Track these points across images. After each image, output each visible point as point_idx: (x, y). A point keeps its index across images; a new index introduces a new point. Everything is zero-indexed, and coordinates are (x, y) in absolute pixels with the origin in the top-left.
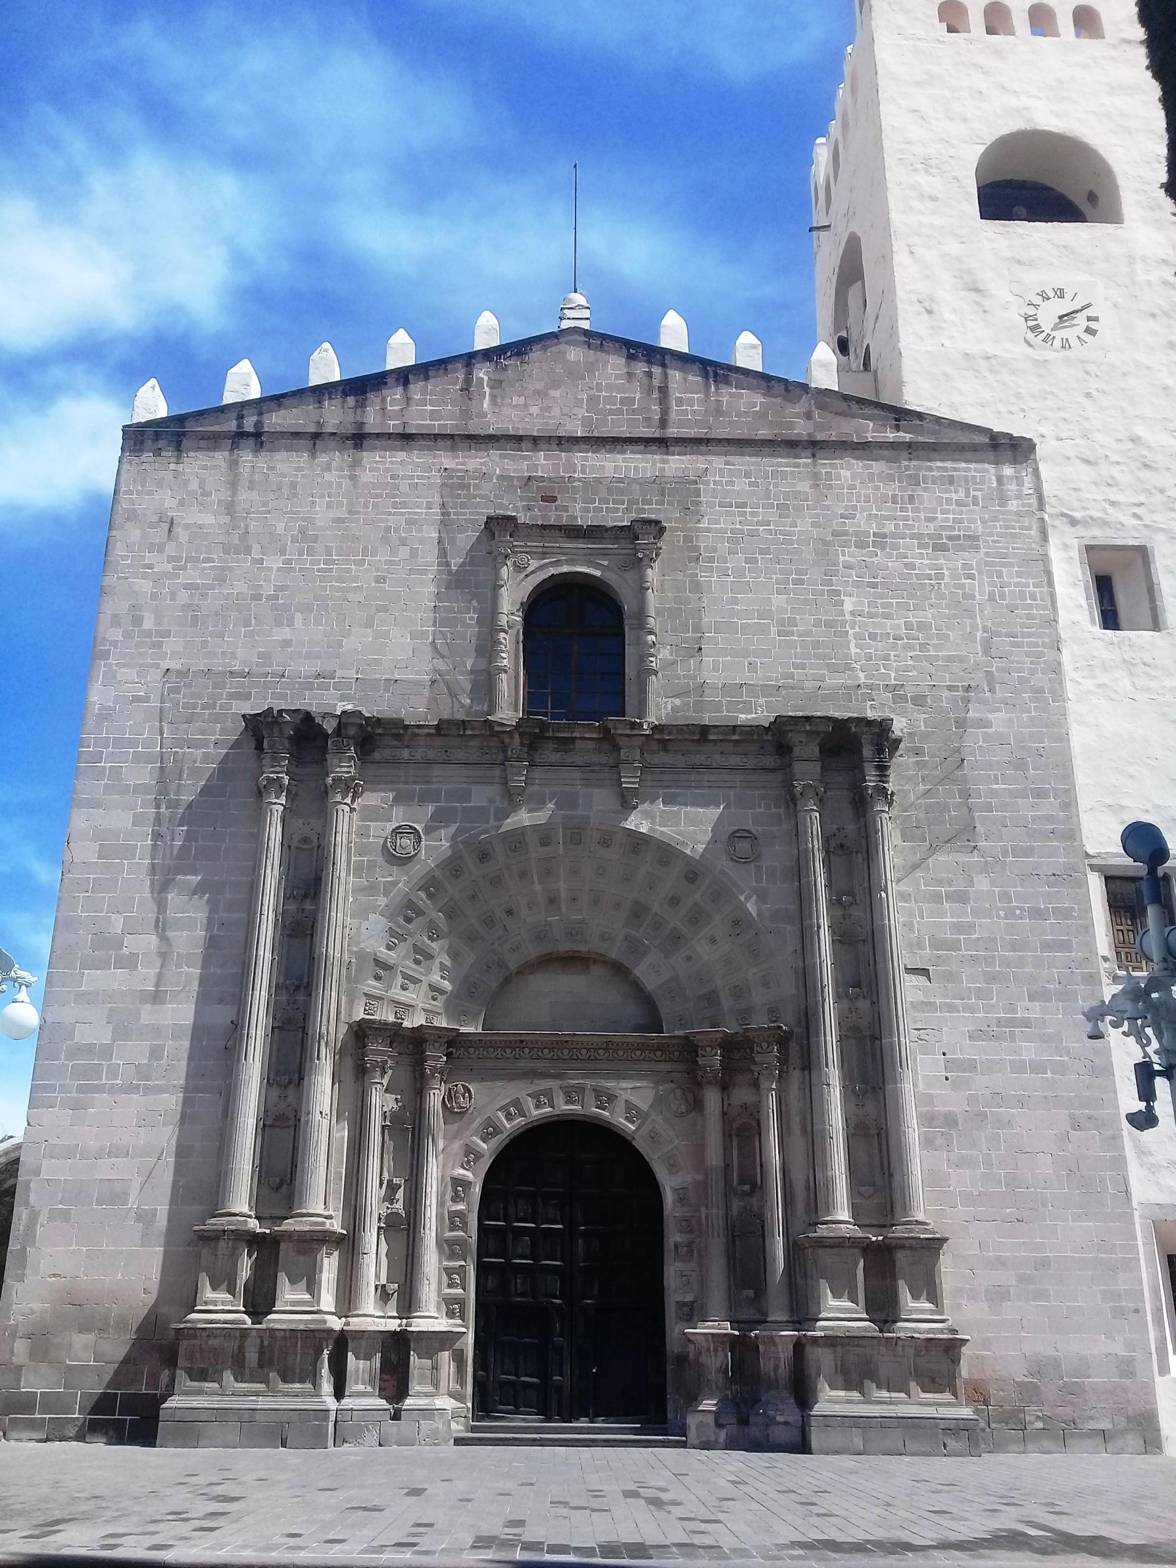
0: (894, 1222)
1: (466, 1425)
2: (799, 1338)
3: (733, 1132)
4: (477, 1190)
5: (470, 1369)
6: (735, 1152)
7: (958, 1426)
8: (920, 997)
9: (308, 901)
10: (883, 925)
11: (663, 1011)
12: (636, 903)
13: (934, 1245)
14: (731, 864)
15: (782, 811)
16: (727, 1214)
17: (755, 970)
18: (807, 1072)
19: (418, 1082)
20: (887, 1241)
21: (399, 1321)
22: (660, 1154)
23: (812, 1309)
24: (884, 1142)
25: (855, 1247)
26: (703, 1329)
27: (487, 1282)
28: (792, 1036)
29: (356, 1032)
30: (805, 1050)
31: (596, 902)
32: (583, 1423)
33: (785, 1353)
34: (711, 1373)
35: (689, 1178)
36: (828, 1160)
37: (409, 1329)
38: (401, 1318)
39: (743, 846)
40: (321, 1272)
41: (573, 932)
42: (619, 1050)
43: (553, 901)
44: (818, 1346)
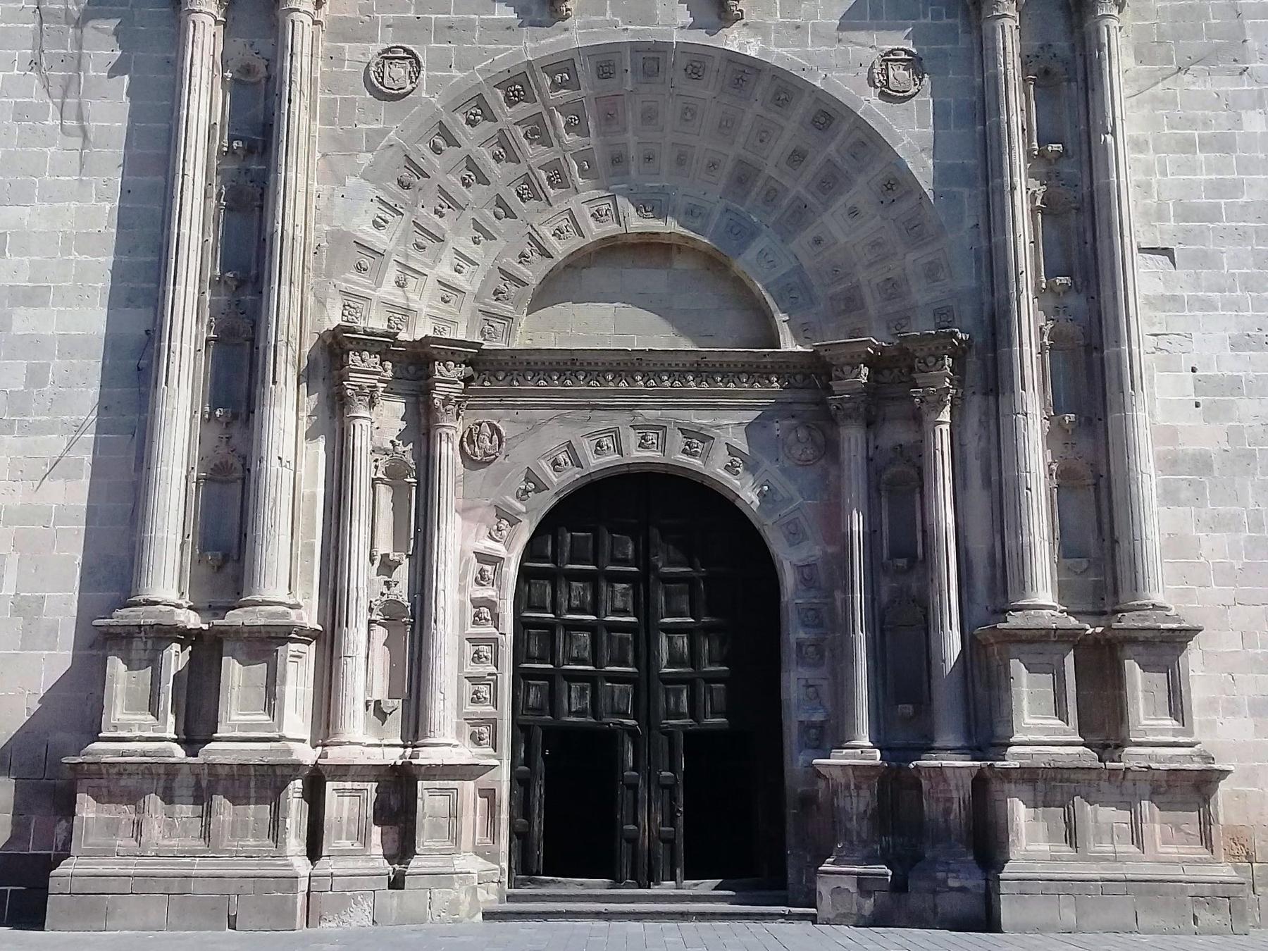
0: (1117, 607)
1: (500, 892)
2: (981, 768)
4: (511, 571)
5: (505, 816)
6: (885, 514)
7: (1214, 891)
8: (1161, 289)
13: (1178, 639)
15: (959, 21)
16: (873, 600)
19: (423, 421)
20: (1109, 634)
21: (402, 750)
22: (776, 517)
23: (1000, 730)
24: (1103, 493)
25: (1064, 642)
26: (838, 759)
27: (528, 695)
28: (970, 347)
29: (330, 346)
30: (990, 364)
32: (667, 887)
33: (960, 793)
34: (851, 819)
35: (817, 551)
36: (1025, 521)
37: (414, 761)
38: (405, 747)
40: (283, 683)
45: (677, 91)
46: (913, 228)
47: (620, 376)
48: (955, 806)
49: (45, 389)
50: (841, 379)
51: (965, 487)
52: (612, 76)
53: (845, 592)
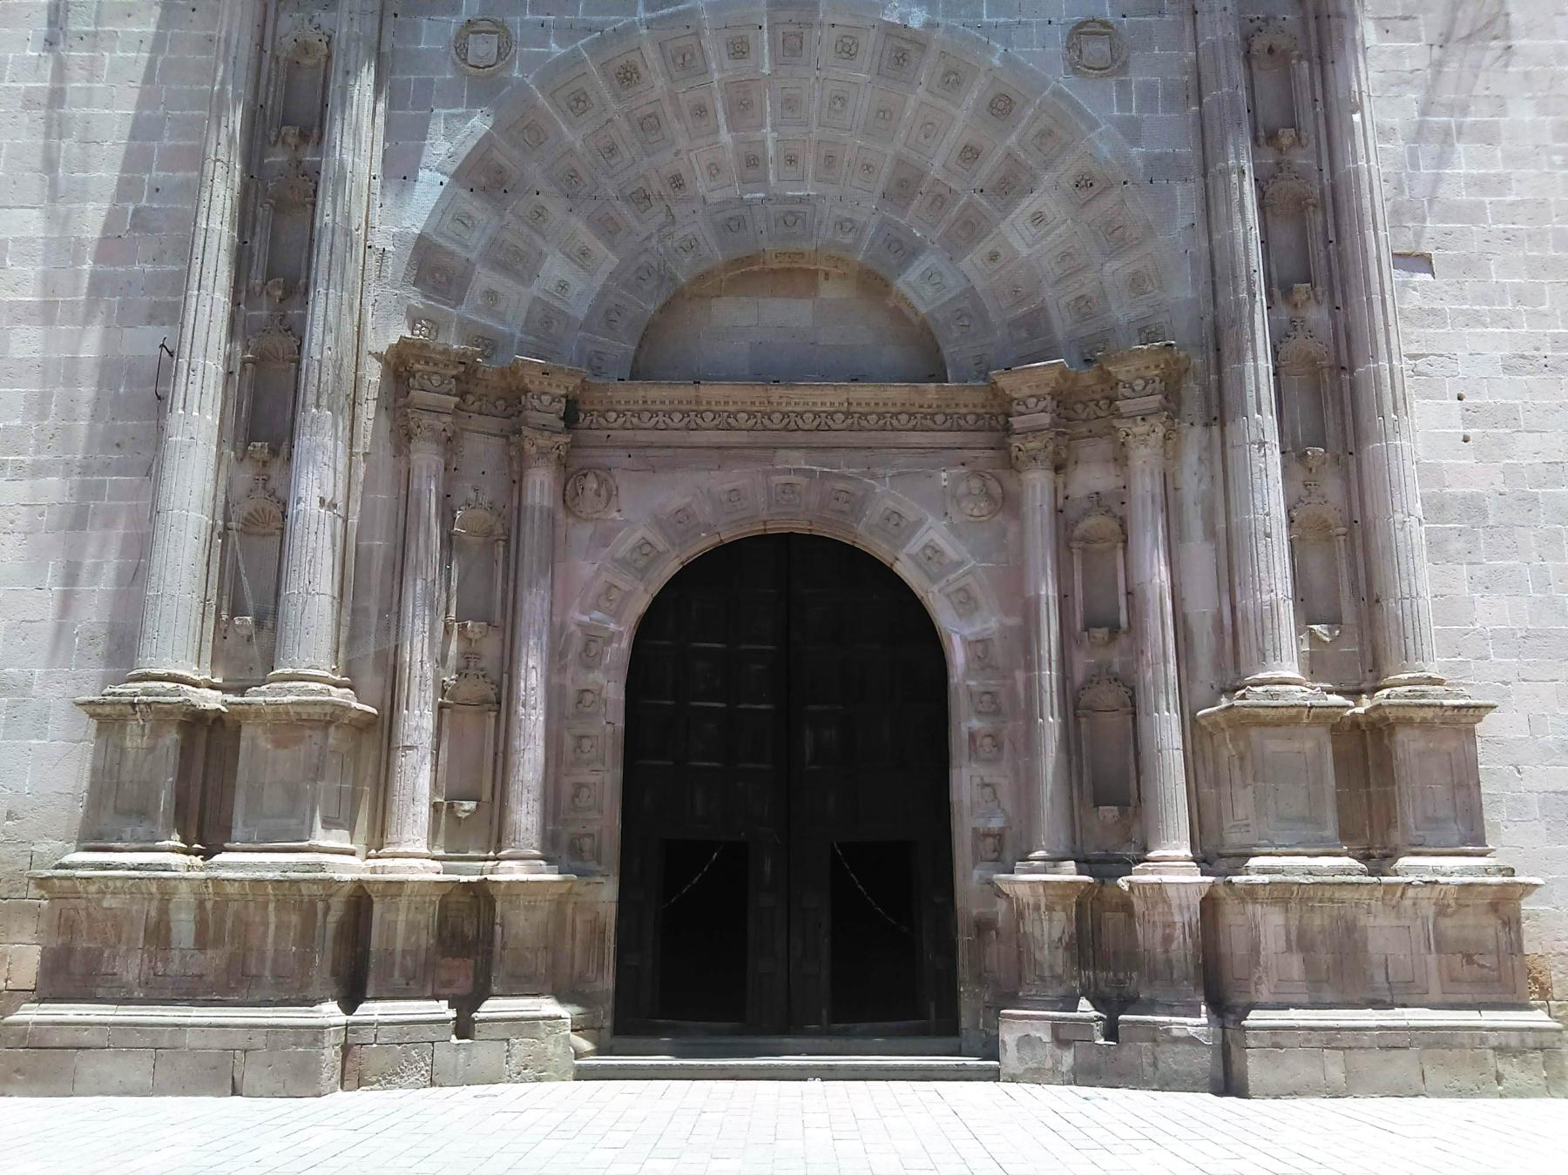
3: (1074, 544)
9: (310, 148)
10: (1357, 172)
11: (947, 351)
12: (900, 162)
14: (1073, 78)
17: (1115, 264)
18: (1216, 429)
19: (515, 468)
30: (1214, 392)
31: (830, 160)
33: (1185, 915)
37: (490, 877)
39: (1097, 49)
41: (790, 219)
42: (871, 414)
43: (753, 162)
44: (1255, 901)
45: (824, 74)
46: (1113, 232)
47: (755, 417)
48: (1178, 933)
49: (46, 422)
50: (1022, 414)
51: (1181, 539)
52: (746, 55)
53: (1029, 667)
